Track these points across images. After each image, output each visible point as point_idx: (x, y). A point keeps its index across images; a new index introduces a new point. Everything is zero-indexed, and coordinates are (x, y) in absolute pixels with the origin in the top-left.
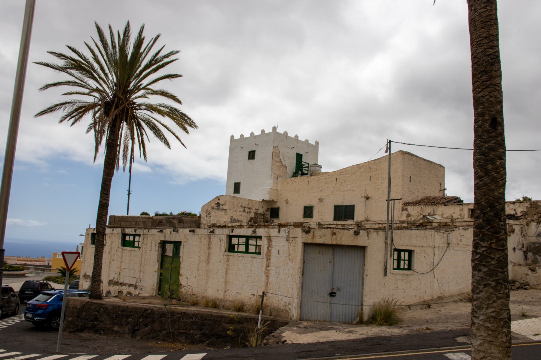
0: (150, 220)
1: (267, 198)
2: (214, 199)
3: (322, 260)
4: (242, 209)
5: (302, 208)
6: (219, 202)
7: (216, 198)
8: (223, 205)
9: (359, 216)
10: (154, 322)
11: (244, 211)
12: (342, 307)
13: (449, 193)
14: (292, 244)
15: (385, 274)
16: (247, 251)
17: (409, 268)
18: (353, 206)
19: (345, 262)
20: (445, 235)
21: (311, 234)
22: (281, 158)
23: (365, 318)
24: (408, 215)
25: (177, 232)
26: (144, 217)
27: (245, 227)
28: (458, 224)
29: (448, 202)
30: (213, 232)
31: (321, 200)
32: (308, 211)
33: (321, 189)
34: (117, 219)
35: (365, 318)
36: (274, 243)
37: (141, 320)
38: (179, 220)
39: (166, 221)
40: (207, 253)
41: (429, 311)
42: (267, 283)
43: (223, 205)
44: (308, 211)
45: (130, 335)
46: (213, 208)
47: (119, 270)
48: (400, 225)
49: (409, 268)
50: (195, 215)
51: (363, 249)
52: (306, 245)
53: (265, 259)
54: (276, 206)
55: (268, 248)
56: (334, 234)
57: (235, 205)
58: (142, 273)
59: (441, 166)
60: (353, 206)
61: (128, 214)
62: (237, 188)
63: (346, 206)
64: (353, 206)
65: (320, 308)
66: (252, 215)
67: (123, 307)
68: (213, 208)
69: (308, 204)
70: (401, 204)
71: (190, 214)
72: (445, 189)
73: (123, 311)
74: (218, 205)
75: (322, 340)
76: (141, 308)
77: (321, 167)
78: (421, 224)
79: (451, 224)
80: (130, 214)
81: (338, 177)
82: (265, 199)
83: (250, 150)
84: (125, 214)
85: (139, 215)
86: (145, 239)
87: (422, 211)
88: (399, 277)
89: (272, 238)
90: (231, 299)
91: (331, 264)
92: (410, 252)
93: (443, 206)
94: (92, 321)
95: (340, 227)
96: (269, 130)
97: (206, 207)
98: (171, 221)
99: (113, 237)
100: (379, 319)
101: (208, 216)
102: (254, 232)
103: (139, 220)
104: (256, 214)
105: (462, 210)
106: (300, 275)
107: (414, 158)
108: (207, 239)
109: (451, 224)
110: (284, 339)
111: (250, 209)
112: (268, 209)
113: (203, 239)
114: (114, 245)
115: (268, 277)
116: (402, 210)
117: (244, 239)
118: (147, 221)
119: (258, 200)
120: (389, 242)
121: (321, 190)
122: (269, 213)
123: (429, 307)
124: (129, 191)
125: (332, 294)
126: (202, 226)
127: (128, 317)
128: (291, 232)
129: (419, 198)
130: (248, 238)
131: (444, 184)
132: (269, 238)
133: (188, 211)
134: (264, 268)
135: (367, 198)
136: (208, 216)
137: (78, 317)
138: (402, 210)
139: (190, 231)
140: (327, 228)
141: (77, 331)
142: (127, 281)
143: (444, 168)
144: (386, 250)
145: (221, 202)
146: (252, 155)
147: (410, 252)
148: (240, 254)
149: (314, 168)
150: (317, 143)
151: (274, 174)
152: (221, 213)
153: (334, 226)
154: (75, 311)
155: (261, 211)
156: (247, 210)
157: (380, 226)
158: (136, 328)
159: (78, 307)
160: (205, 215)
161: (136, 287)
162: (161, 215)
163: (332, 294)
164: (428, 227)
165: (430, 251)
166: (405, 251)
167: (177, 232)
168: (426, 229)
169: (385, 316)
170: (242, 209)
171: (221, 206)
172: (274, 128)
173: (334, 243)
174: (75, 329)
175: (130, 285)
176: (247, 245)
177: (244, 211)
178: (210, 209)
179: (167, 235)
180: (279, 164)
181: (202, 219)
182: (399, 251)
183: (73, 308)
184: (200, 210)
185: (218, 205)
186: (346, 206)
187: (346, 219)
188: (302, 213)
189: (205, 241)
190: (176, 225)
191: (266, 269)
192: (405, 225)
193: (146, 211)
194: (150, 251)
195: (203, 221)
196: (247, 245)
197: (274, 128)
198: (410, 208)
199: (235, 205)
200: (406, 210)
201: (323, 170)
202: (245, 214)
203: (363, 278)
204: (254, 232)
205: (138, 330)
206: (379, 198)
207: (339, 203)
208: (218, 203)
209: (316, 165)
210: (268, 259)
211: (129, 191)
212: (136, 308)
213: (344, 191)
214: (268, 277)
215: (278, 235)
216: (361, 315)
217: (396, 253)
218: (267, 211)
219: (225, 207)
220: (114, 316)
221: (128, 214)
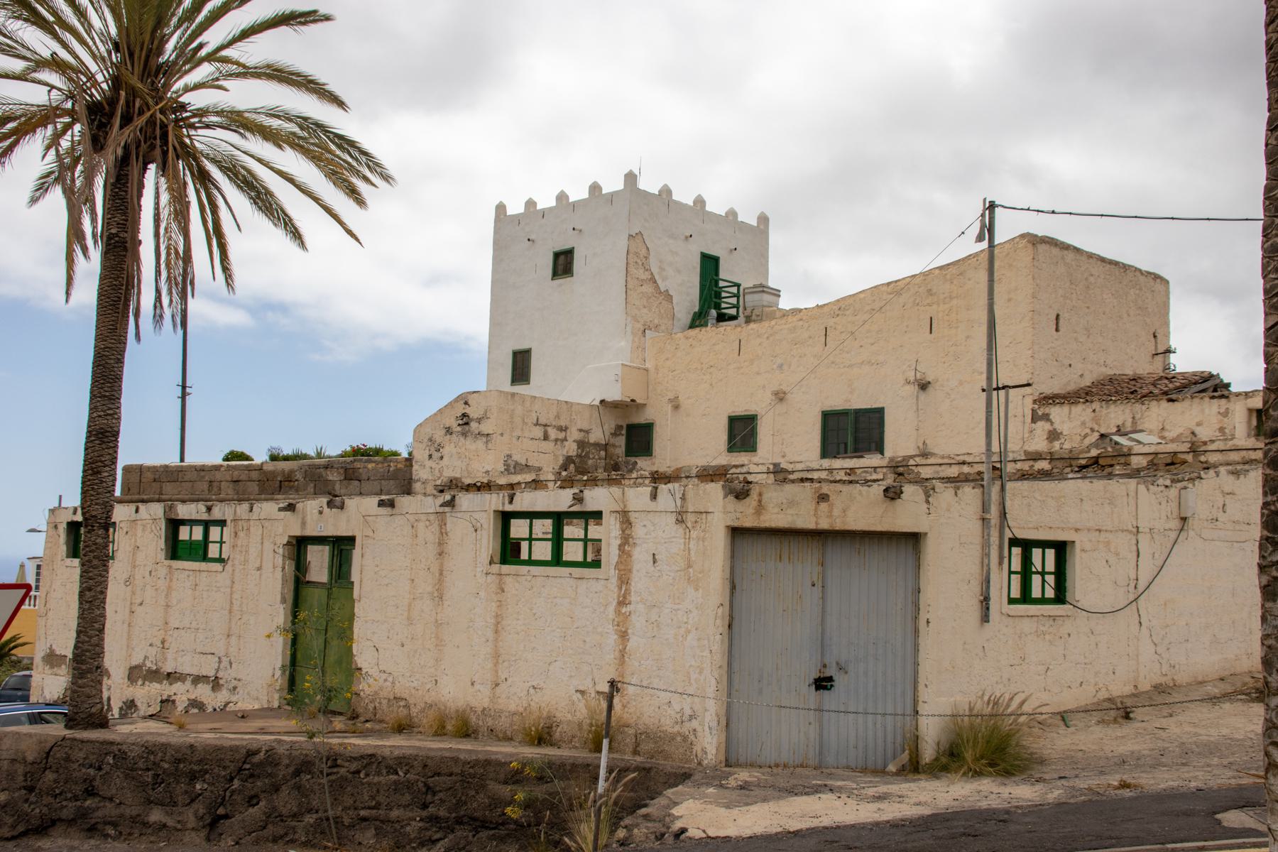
0: (255, 475)
1: (614, 395)
2: (451, 405)
3: (790, 575)
4: (538, 432)
5: (724, 423)
6: (468, 410)
7: (456, 400)
8: (479, 421)
9: (898, 441)
10: (276, 789)
11: (546, 438)
12: (853, 723)
13: (1182, 363)
14: (694, 534)
15: (985, 618)
16: (557, 559)
17: (1060, 598)
19: (861, 584)
20: (1173, 492)
21: (751, 501)
22: (655, 270)
23: (928, 754)
24: (1053, 435)
25: (342, 507)
26: (235, 467)
27: (551, 485)
28: (1213, 458)
29: (1180, 389)
30: (451, 503)
31: (780, 397)
32: (742, 431)
33: (779, 361)
34: (149, 476)
35: (928, 754)
36: (638, 531)
37: (236, 783)
40: (435, 569)
41: (1127, 729)
42: (623, 653)
43: (479, 421)
44: (742, 431)
45: (203, 833)
46: (449, 431)
47: (161, 635)
48: (1025, 466)
49: (1060, 598)
50: (395, 454)
51: (914, 539)
52: (736, 532)
53: (614, 581)
54: (641, 419)
55: (621, 547)
56: (823, 498)
57: (518, 420)
58: (233, 640)
59: (1156, 277)
60: (880, 411)
61: (182, 460)
62: (521, 366)
63: (858, 412)
64: (880, 411)
65: (787, 727)
66: (571, 449)
67: (178, 749)
68: (449, 431)
69: (740, 410)
70: (1029, 401)
71: (378, 451)
72: (1168, 351)
73: (179, 761)
74: (465, 420)
75: (795, 825)
76: (234, 749)
77: (776, 293)
78: (1095, 461)
79: (1189, 457)
80: (192, 459)
81: (831, 322)
82: (609, 398)
83: (557, 249)
84: (172, 459)
85: (218, 460)
86: (241, 534)
87: (1096, 420)
88: (1027, 626)
89: (632, 516)
90: (513, 707)
91: (817, 591)
92: (1061, 549)
93: (1164, 404)
94: (76, 798)
95: (841, 476)
96: (612, 184)
97: (428, 430)
98: (320, 476)
99: (139, 533)
100: (969, 755)
101: (436, 455)
102: (578, 499)
103: (218, 476)
104: (581, 444)
105: (1226, 414)
106: (721, 625)
107: (1070, 256)
108: (435, 528)
109: (1189, 457)
110: (678, 825)
111: (562, 429)
112: (619, 427)
113: (421, 525)
114: (140, 557)
115: (624, 636)
116: (1034, 420)
117: (548, 524)
118: (243, 477)
119: (588, 402)
120: (994, 517)
121: (781, 366)
122: (621, 441)
123: (1127, 716)
124: (184, 387)
125: (823, 683)
126: (417, 486)
127: (193, 777)
128: (690, 495)
129: (1087, 382)
130: (559, 518)
131: (1167, 335)
132: (625, 518)
133: (372, 444)
134: (611, 609)
135: (924, 386)
136: (436, 455)
137: (31, 789)
138: (1035, 418)
139: (381, 504)
140: (802, 480)
141: (24, 834)
142: (187, 665)
143: (1167, 282)
144: (986, 545)
145: (473, 412)
146: (563, 263)
147: (1061, 549)
148: (535, 570)
149: (757, 297)
150: (764, 220)
151: (635, 319)
152: (473, 447)
153: (823, 475)
154: (21, 769)
155: (597, 436)
156: (553, 433)
157: (966, 469)
158: (221, 811)
159: (30, 758)
160: (427, 453)
161: (216, 684)
162: (286, 458)
163: (823, 683)
164: (1118, 470)
165: (1124, 543)
166: (1044, 544)
167: (342, 507)
168: (1110, 476)
169: (988, 746)
170: (538, 432)
171: (473, 425)
172: (631, 178)
173: (824, 525)
174: (21, 828)
175: (198, 679)
176: (558, 540)
177: (546, 438)
178: (439, 435)
179: (309, 518)
180: (648, 289)
181: (415, 467)
182: (1027, 546)
183: (13, 761)
184: (410, 439)
185: (465, 420)
186: (859, 413)
187: (858, 451)
188: (725, 437)
189: (428, 533)
190: (337, 486)
191: (618, 612)
192: (1044, 465)
193: (238, 449)
194: (259, 569)
195: (421, 472)
196: (558, 540)
197: (631, 178)
198: (1057, 413)
199: (518, 420)
200: (1046, 417)
201: (785, 303)
202: (548, 446)
203: (916, 631)
204: (578, 499)
205: (226, 817)
206: (961, 383)
207: (838, 401)
208: (464, 415)
209: (762, 289)
210: (624, 580)
211: (184, 387)
212: (219, 749)
213: (850, 366)
214: (624, 636)
215: (652, 506)
216: (915, 742)
217: (1016, 551)
218: (614, 435)
219: (486, 427)
220: (149, 777)
221: (182, 460)
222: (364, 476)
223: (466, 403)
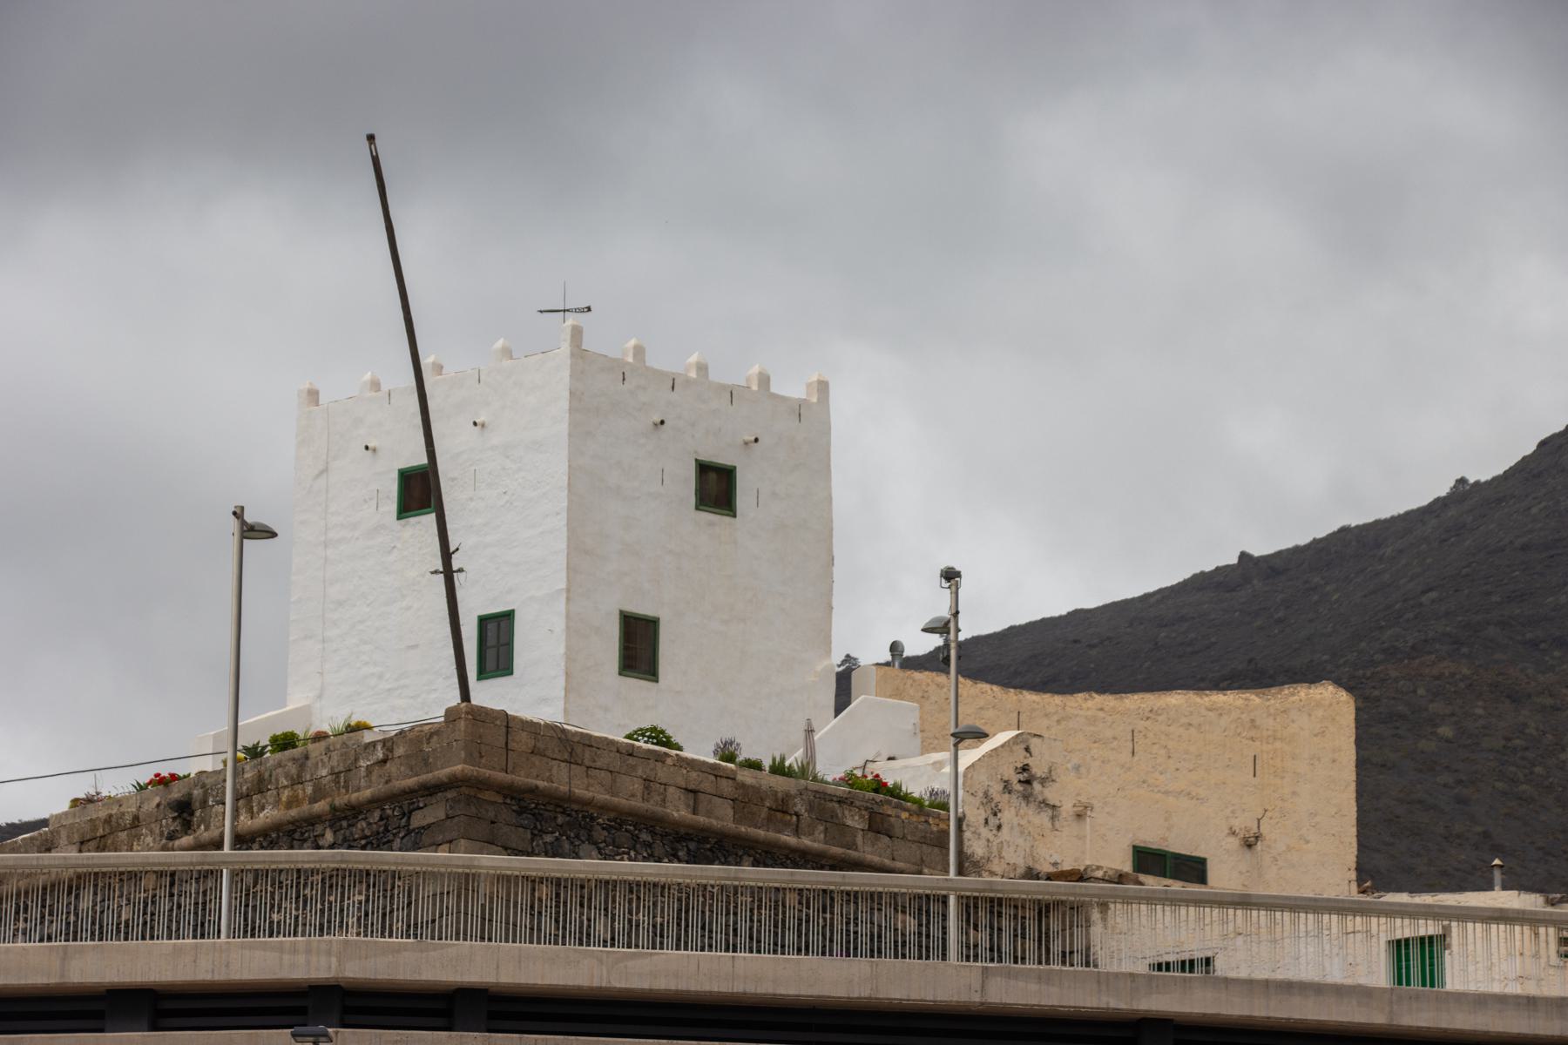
6: (1029, 761)
8: (1043, 781)
33: (1075, 761)
38: (872, 814)
39: (810, 809)
62: (639, 645)
68: (1007, 787)
83: (706, 457)
97: (982, 779)
98: (834, 815)
118: (707, 784)
121: (1077, 768)
136: (993, 821)
145: (1038, 770)
146: (716, 488)
171: (1037, 786)
190: (859, 840)
206: (1289, 849)
208: (1025, 768)
213: (1167, 793)
219: (1051, 794)
222: (898, 831)
223: (1027, 749)
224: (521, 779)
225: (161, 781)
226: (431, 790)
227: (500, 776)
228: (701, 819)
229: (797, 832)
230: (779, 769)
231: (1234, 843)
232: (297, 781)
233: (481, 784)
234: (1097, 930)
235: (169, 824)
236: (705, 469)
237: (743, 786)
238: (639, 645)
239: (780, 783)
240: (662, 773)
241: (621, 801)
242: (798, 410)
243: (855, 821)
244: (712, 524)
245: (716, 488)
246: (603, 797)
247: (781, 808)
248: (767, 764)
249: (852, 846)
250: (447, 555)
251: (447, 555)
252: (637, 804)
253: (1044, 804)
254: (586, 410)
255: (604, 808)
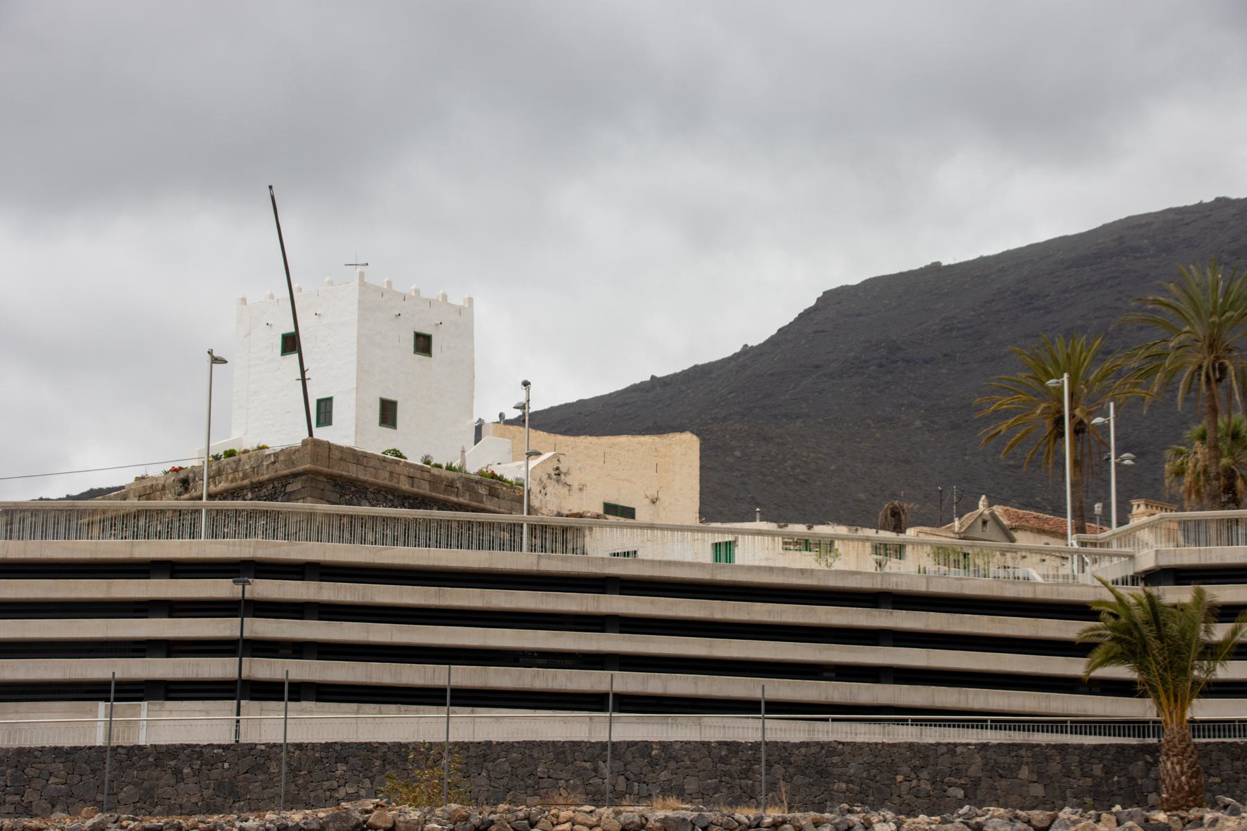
18: (633, 510)
34: (337, 455)
39: (463, 485)
62: (388, 413)
68: (549, 477)
97: (539, 473)
145: (563, 469)
146: (423, 344)
219: (568, 480)
224: (335, 471)
225: (175, 470)
226: (295, 475)
227: (326, 470)
228: (415, 490)
229: (457, 495)
230: (449, 468)
231: (647, 501)
232: (235, 471)
233: (318, 473)
234: (587, 539)
235: (179, 488)
236: (418, 336)
237: (433, 475)
238: (388, 413)
239: (450, 474)
240: (398, 469)
241: (380, 481)
242: (460, 311)
243: (483, 491)
244: (612, 446)
245: (423, 344)
246: (371, 479)
247: (451, 485)
248: (444, 466)
249: (482, 502)
250: (303, 372)
251: (303, 372)
252: (387, 482)
253: (566, 484)
254: (365, 309)
255: (372, 484)
